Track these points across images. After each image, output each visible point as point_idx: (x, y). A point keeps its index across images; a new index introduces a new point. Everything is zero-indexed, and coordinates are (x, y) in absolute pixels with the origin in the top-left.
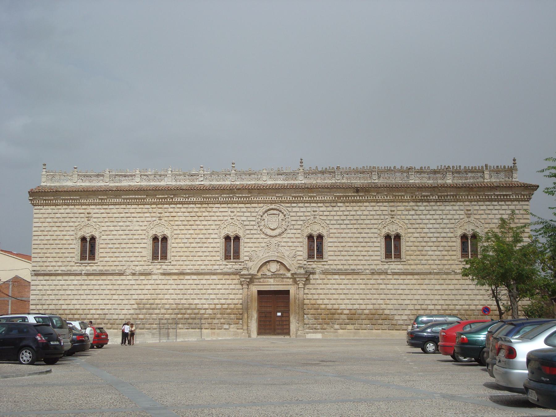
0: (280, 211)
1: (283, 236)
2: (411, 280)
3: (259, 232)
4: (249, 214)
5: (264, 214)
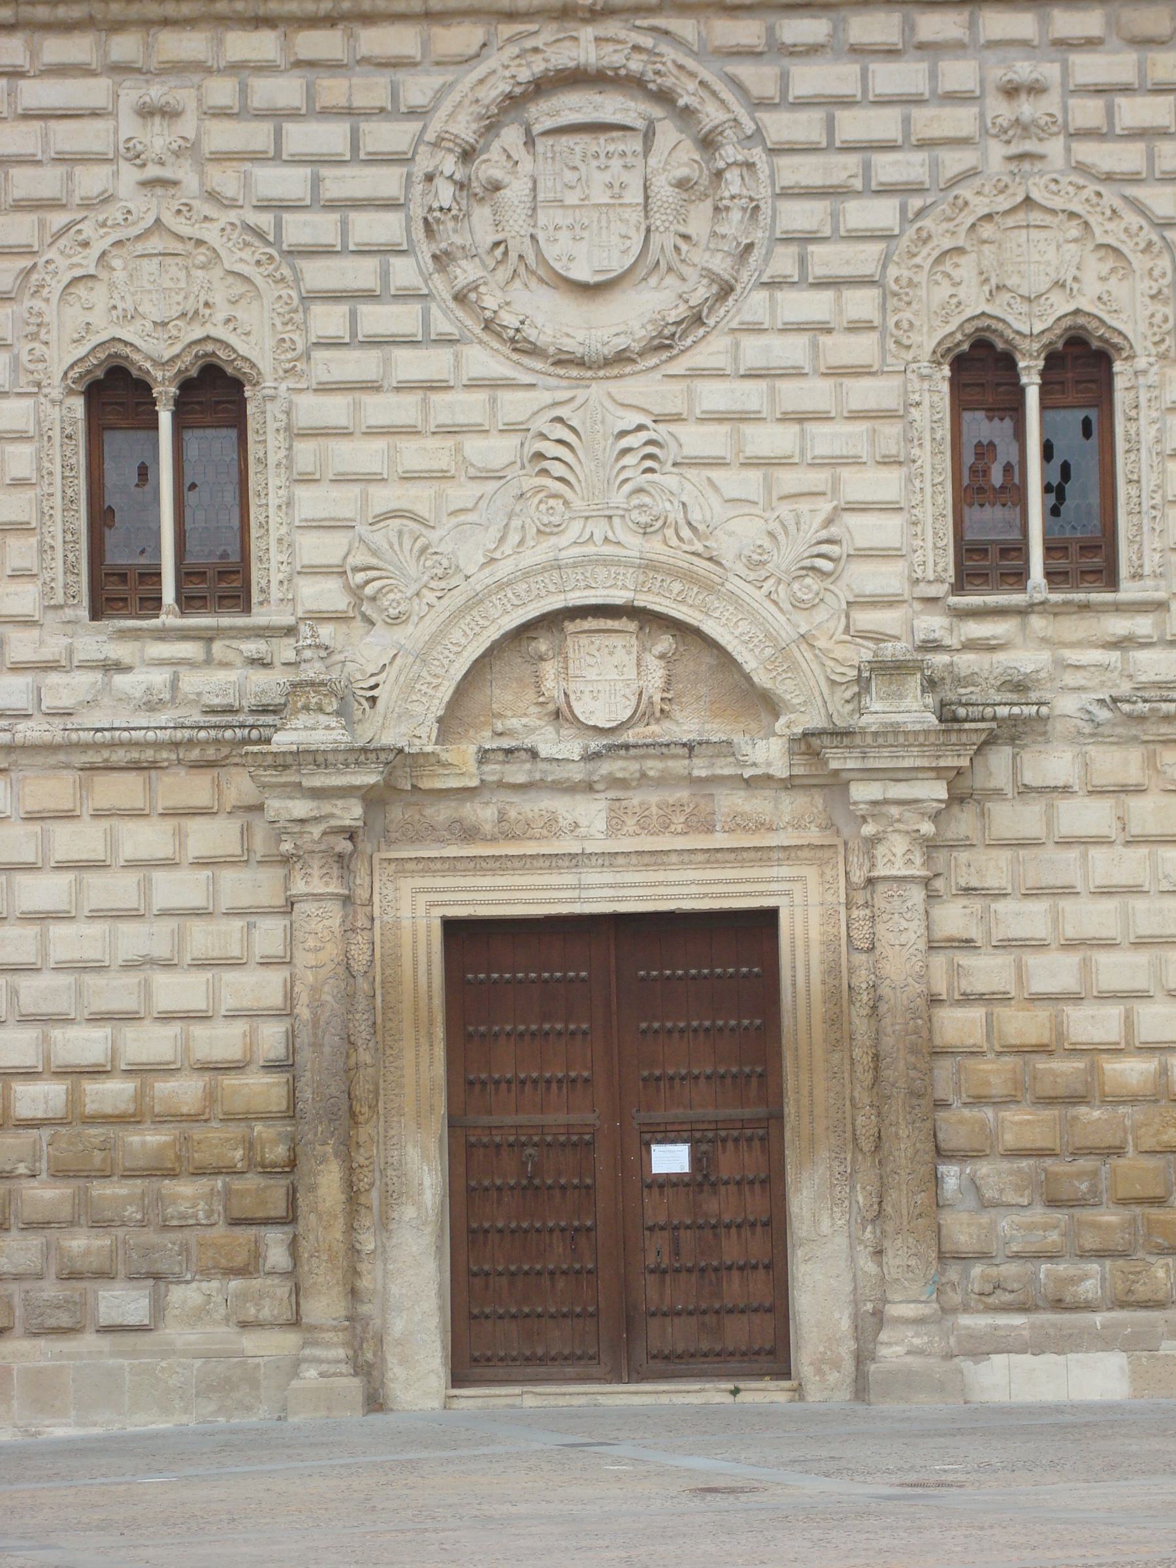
0: (664, 97)
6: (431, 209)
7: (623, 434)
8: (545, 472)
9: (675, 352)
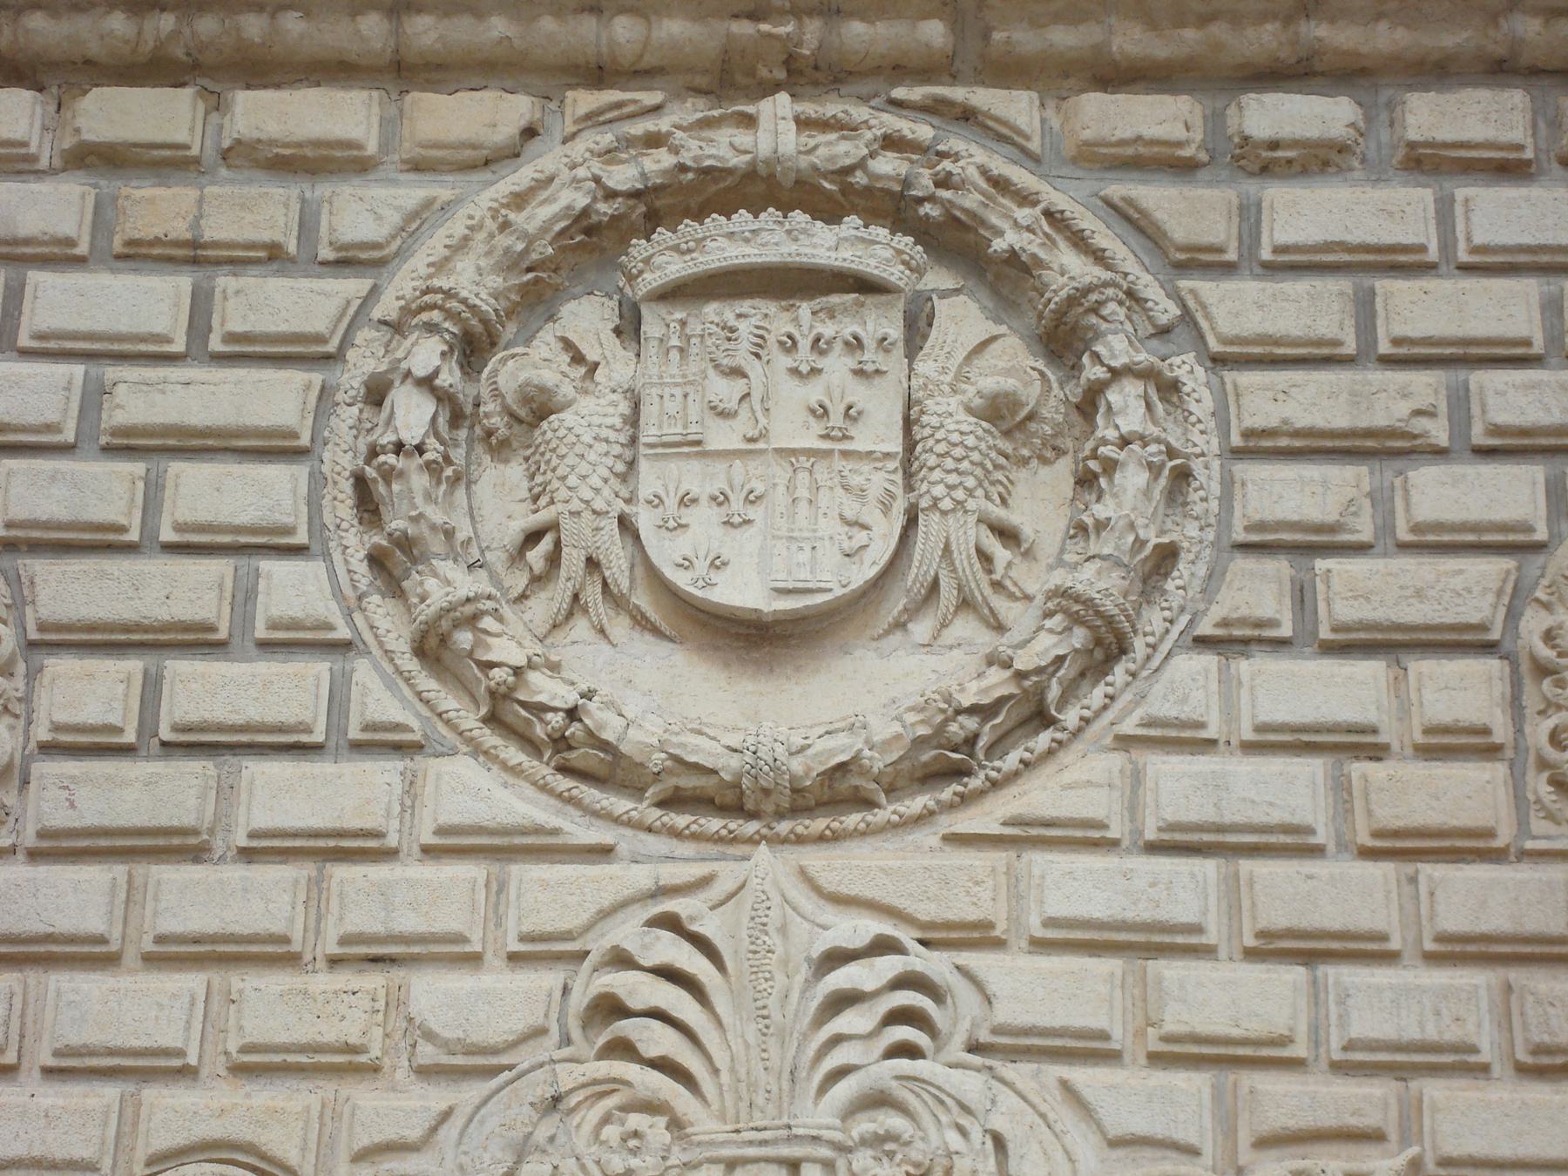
1: (1040, 796)
3: (378, 699)
4: (152, 302)
5: (537, 295)
6: (373, 452)
7: (837, 958)
8: (623, 1049)
9: (975, 783)
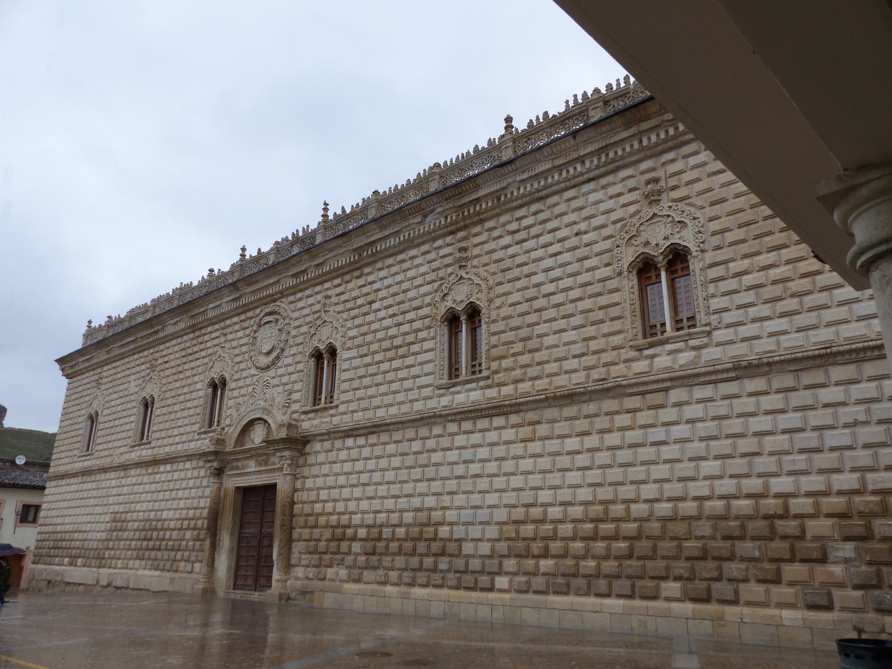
2: (502, 431)
